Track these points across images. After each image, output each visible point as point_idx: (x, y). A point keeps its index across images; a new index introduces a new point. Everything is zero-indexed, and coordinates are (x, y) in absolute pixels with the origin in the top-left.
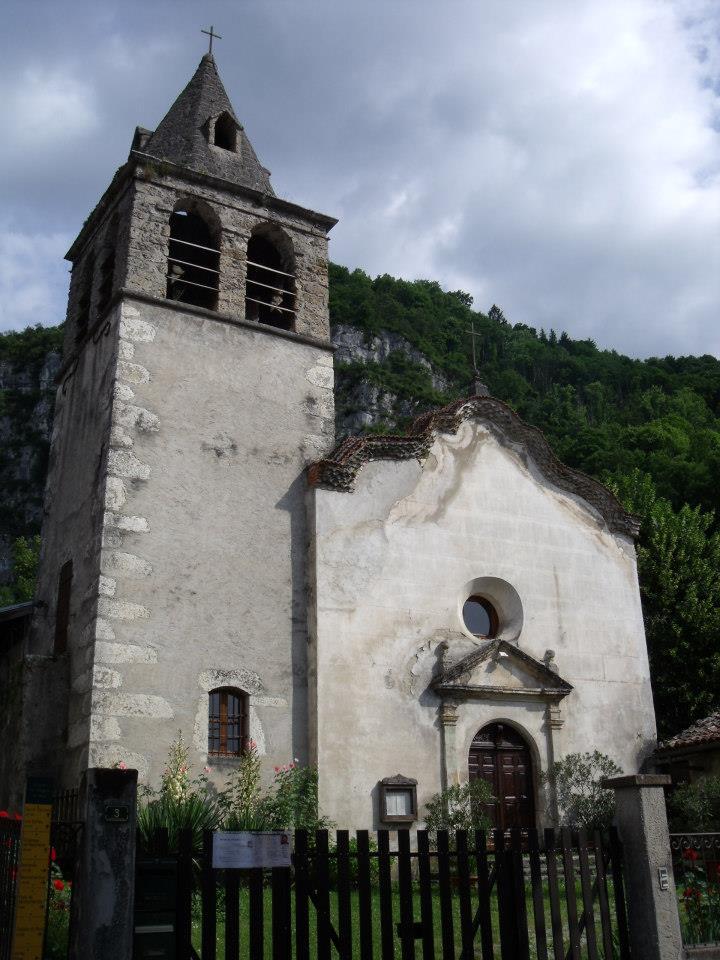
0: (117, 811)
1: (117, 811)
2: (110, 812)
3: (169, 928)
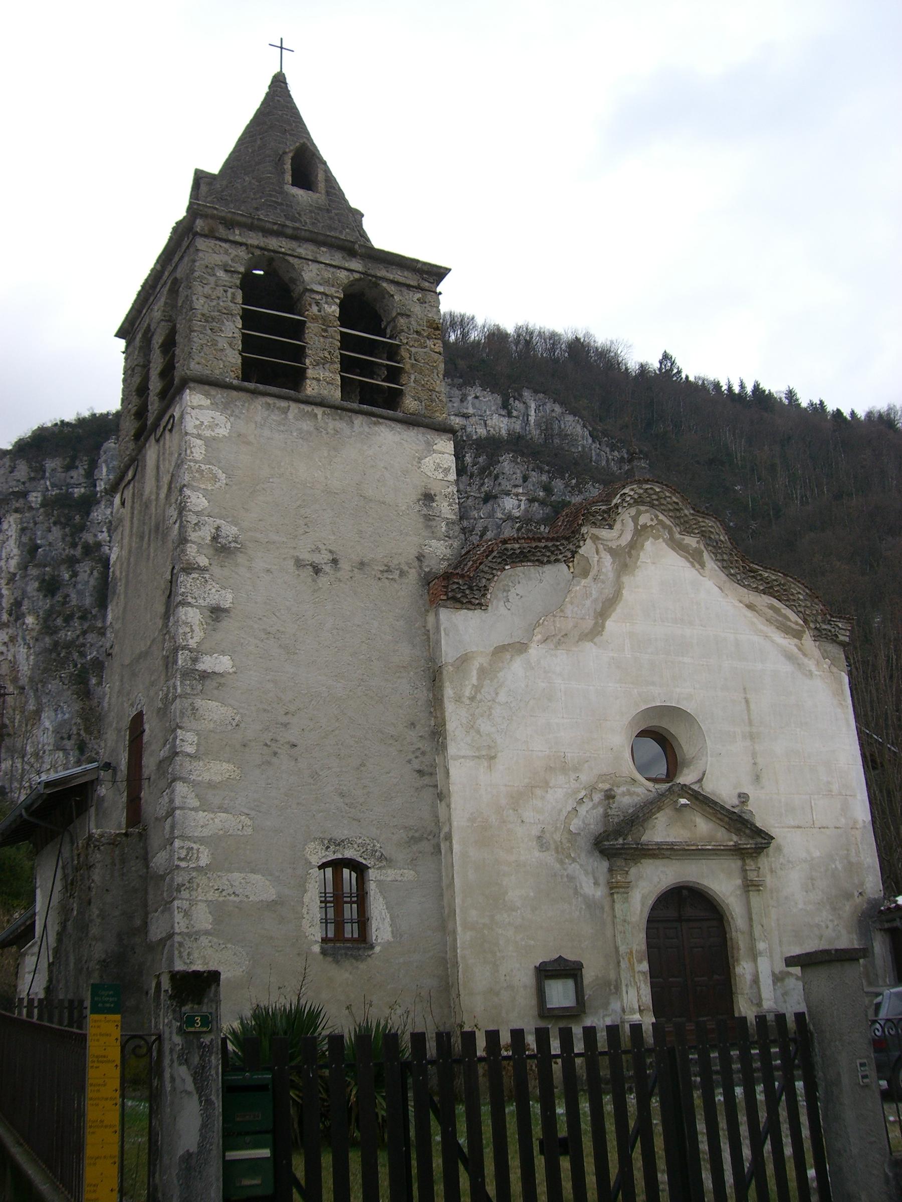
2: (191, 1021)
3: (266, 1153)
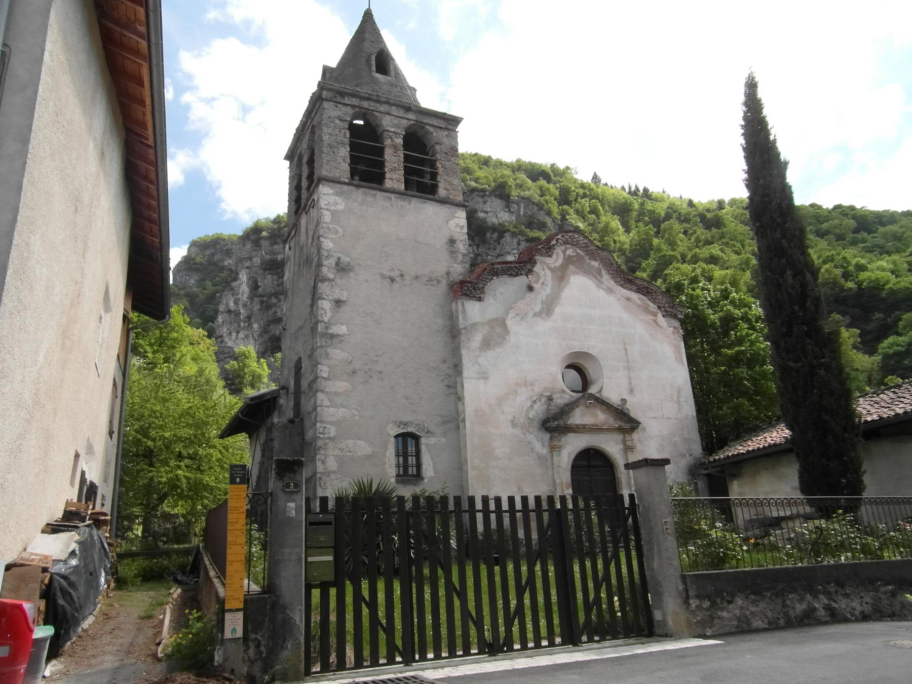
0: (292, 485)
1: (292, 485)
2: (288, 486)
3: (330, 558)
